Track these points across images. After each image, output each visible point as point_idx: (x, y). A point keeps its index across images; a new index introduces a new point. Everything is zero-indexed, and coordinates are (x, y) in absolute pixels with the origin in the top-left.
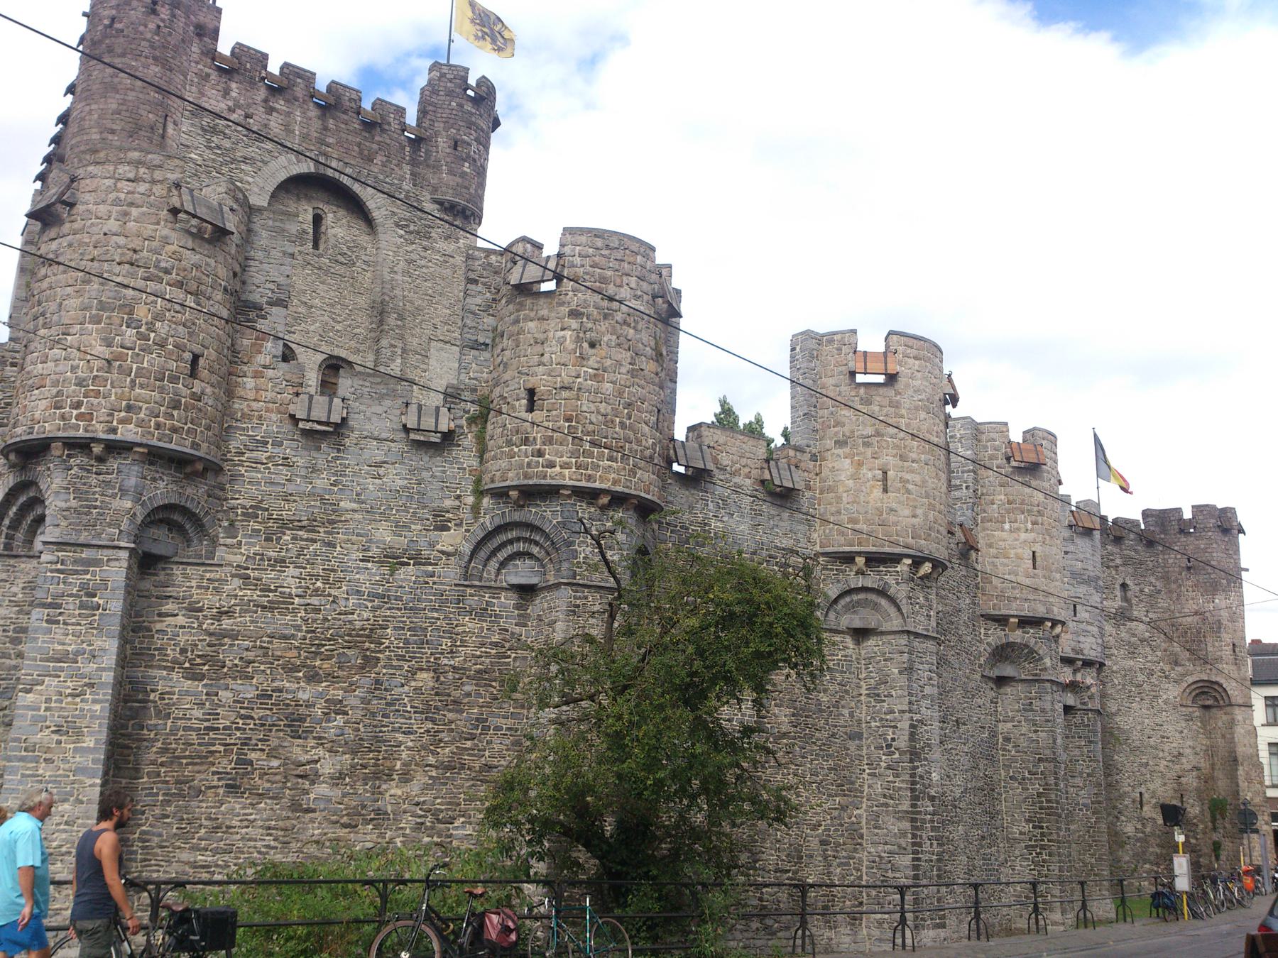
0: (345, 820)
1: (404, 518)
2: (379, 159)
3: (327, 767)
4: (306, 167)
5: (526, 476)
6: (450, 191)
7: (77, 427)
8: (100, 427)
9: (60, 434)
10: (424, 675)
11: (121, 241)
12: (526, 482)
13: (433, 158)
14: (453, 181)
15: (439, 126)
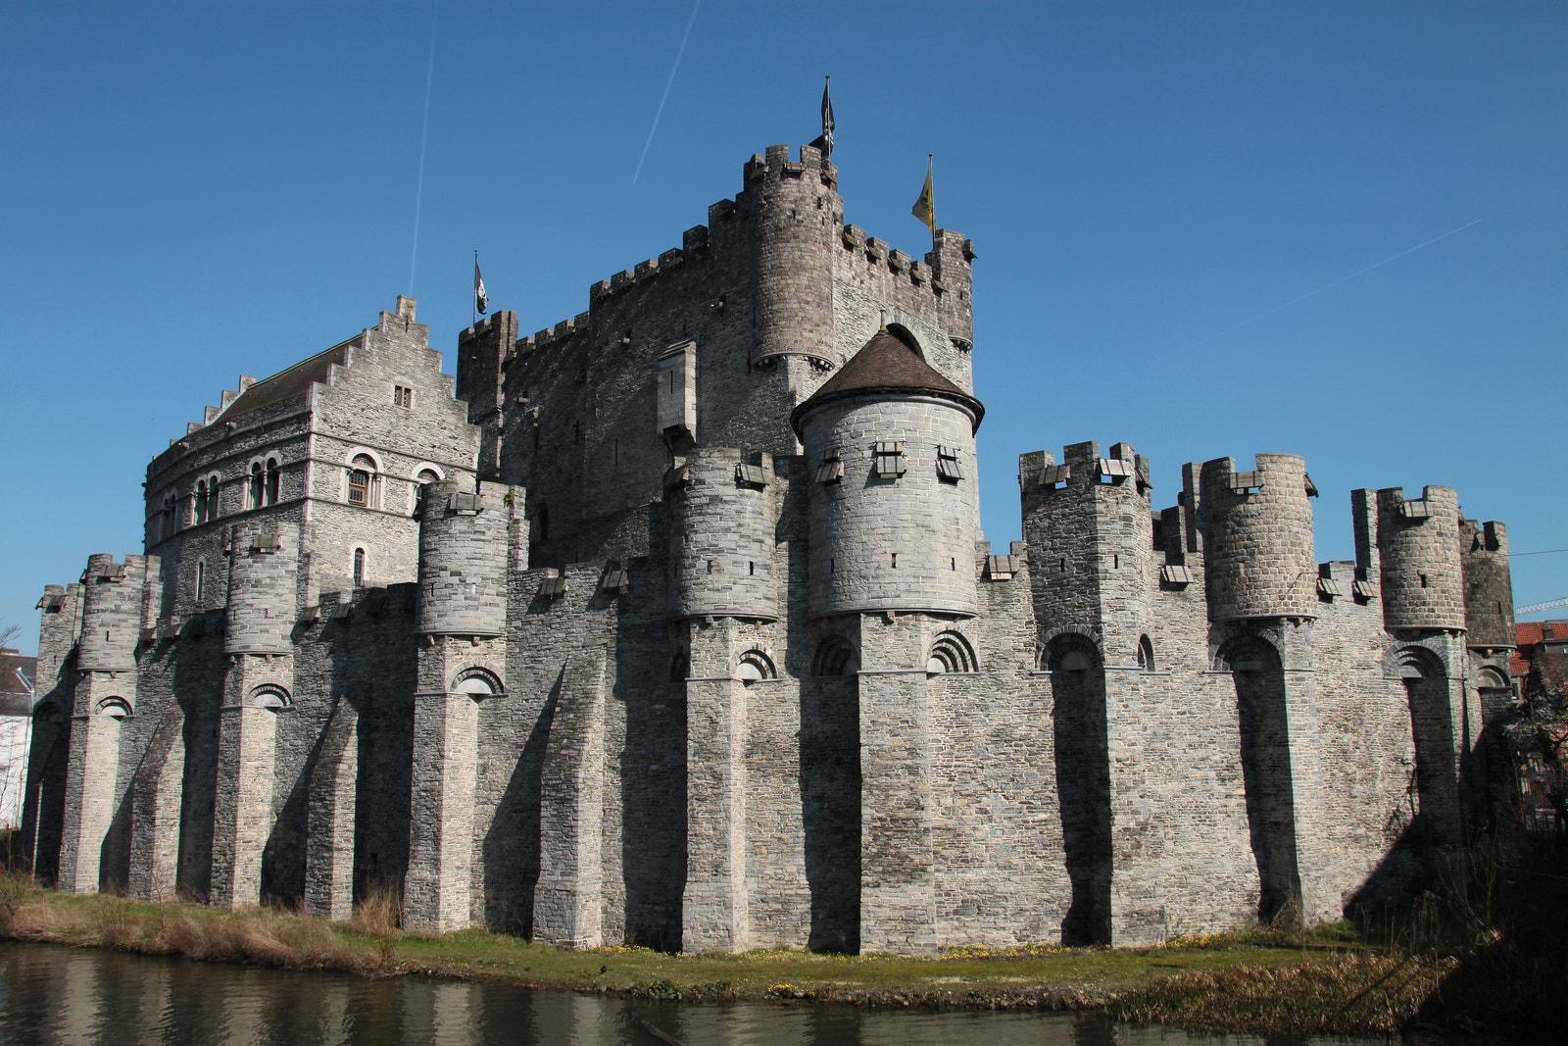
0: (1367, 801)
1: (1361, 643)
2: (923, 308)
3: (1358, 777)
4: (889, 320)
5: (1426, 622)
6: (961, 332)
7: (1292, 610)
8: (1301, 609)
9: (1287, 614)
10: (1380, 727)
11: (1293, 507)
12: (1427, 626)
13: (947, 306)
14: (962, 323)
15: (949, 280)
